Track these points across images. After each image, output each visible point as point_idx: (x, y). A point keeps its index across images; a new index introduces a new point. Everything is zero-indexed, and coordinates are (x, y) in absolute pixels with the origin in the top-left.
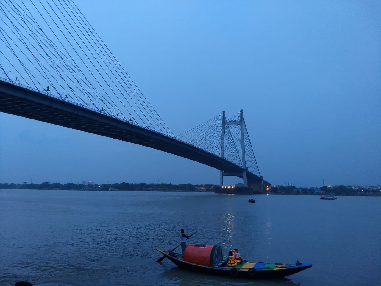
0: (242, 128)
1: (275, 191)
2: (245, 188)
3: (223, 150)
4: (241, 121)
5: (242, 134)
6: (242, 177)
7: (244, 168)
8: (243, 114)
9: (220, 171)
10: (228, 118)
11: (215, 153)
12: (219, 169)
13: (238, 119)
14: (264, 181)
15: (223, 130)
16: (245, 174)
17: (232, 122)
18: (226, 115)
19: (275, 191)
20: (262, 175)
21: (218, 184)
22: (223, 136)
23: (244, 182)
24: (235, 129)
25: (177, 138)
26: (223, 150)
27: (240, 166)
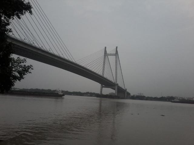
0: (116, 58)
1: (133, 98)
2: (116, 96)
3: (103, 72)
4: (116, 53)
5: (116, 62)
6: (114, 89)
7: (116, 83)
8: (118, 50)
9: (100, 84)
10: (108, 52)
11: (99, 74)
12: (100, 84)
13: (115, 53)
14: (127, 92)
15: (105, 58)
16: (116, 87)
17: (111, 55)
18: (107, 49)
19: (133, 98)
20: (126, 88)
21: (98, 92)
22: (104, 62)
23: (115, 92)
24: (112, 59)
25: (77, 62)
26: (103, 72)
27: (114, 82)
